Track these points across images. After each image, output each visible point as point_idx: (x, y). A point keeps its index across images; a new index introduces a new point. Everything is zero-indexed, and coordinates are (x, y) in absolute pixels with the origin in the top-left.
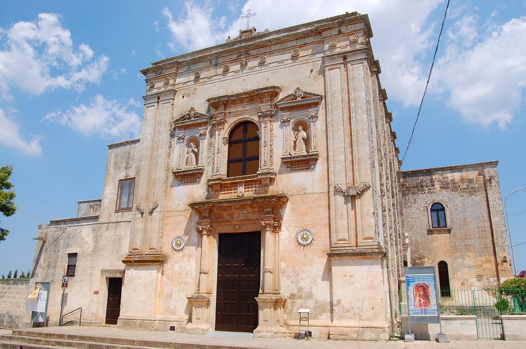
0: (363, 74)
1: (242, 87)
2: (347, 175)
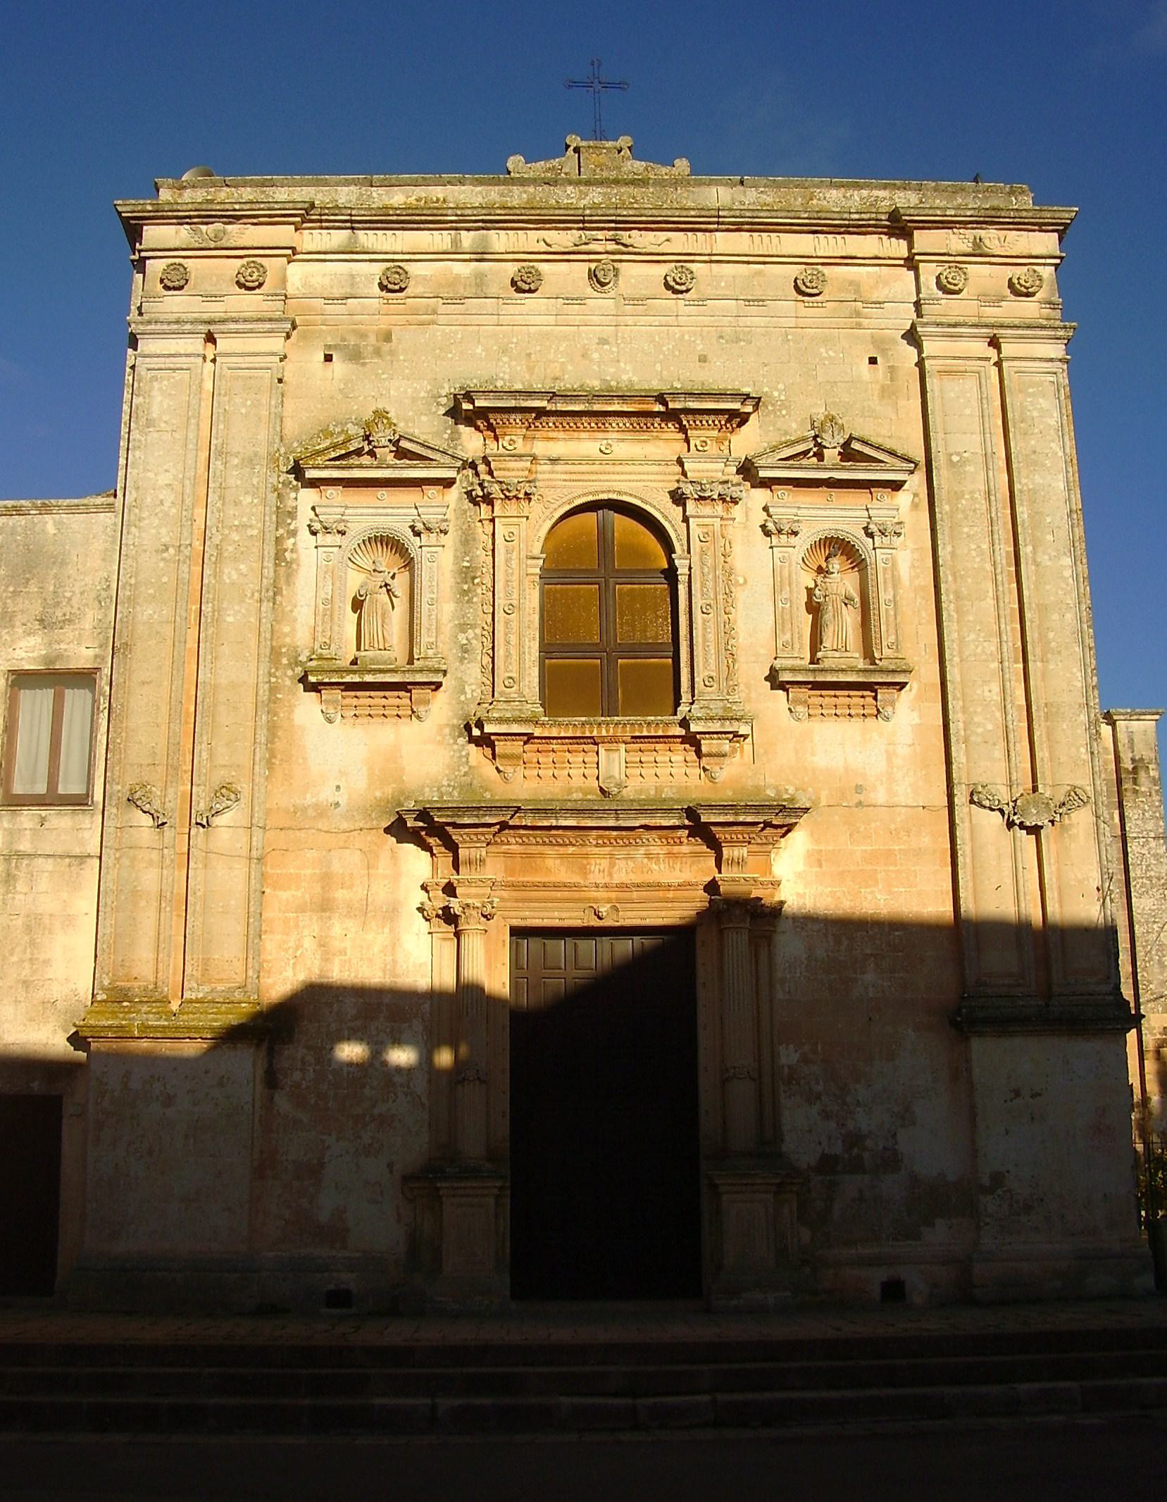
0: (1056, 414)
1: (595, 367)
2: (1012, 754)
